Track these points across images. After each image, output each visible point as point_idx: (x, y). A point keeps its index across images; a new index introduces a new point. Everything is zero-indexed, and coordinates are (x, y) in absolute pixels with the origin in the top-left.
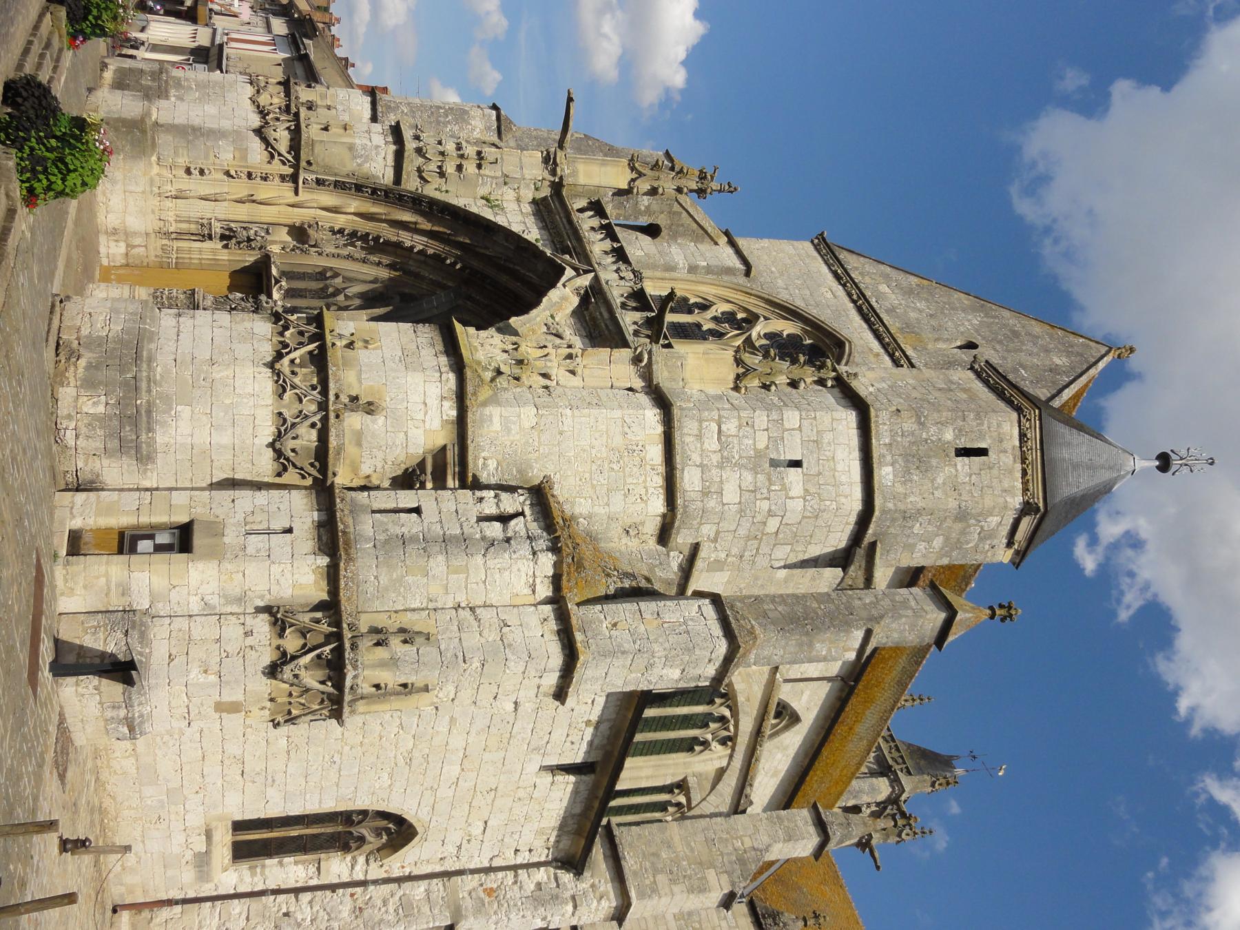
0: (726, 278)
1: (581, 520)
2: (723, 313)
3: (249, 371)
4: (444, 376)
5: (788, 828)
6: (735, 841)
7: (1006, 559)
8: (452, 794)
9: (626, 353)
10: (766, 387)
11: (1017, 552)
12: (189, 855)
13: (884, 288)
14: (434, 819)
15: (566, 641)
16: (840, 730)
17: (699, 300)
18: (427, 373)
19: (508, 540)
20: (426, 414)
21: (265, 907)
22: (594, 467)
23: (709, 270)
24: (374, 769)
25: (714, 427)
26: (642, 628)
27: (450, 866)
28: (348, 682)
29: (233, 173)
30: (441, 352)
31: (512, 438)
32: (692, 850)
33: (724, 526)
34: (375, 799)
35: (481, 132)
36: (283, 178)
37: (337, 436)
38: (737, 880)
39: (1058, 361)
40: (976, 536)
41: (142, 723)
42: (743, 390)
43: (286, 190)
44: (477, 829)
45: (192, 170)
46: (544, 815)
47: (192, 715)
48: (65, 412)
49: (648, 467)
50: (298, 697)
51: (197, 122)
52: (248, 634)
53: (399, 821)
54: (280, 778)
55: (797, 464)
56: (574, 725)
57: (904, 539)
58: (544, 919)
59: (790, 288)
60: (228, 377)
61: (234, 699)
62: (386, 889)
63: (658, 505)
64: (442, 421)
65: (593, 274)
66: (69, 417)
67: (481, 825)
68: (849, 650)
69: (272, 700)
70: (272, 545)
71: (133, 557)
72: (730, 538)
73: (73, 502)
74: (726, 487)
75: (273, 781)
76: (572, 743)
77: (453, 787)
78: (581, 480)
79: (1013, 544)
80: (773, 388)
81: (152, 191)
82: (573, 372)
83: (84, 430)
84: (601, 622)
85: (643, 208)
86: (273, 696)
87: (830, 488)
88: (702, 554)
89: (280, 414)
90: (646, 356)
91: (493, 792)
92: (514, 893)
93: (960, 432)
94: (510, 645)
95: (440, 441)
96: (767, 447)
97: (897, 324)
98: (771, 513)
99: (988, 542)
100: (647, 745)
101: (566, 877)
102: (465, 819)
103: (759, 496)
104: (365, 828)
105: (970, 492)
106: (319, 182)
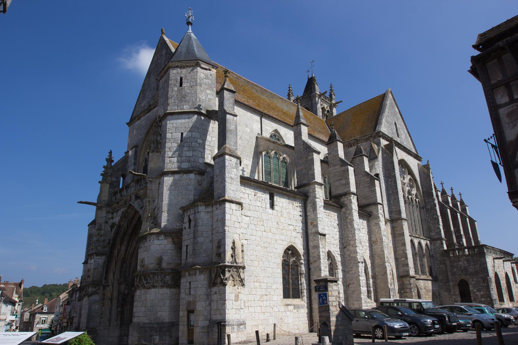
0: (138, 154)
1: (196, 198)
7: (215, 71)
10: (161, 143)
11: (213, 68)
12: (295, 311)
13: (143, 105)
17: (144, 161)
20: (163, 244)
22: (180, 194)
26: (220, 180)
28: (230, 264)
29: (102, 305)
34: (278, 257)
36: (104, 288)
37: (168, 270)
39: (164, 53)
40: (207, 80)
41: (240, 322)
43: (109, 289)
44: (292, 227)
46: (287, 208)
47: (238, 308)
51: (86, 315)
52: (216, 293)
54: (269, 285)
56: (256, 200)
57: (207, 102)
63: (192, 176)
64: (165, 239)
65: (131, 195)
68: (233, 119)
69: (235, 285)
75: (270, 286)
77: (276, 235)
81: (108, 329)
82: (154, 201)
85: (116, 179)
89: (161, 286)
93: (175, 85)
94: (222, 219)
96: (177, 143)
97: (152, 101)
99: (209, 76)
102: (288, 231)
105: (193, 82)
106: (106, 278)
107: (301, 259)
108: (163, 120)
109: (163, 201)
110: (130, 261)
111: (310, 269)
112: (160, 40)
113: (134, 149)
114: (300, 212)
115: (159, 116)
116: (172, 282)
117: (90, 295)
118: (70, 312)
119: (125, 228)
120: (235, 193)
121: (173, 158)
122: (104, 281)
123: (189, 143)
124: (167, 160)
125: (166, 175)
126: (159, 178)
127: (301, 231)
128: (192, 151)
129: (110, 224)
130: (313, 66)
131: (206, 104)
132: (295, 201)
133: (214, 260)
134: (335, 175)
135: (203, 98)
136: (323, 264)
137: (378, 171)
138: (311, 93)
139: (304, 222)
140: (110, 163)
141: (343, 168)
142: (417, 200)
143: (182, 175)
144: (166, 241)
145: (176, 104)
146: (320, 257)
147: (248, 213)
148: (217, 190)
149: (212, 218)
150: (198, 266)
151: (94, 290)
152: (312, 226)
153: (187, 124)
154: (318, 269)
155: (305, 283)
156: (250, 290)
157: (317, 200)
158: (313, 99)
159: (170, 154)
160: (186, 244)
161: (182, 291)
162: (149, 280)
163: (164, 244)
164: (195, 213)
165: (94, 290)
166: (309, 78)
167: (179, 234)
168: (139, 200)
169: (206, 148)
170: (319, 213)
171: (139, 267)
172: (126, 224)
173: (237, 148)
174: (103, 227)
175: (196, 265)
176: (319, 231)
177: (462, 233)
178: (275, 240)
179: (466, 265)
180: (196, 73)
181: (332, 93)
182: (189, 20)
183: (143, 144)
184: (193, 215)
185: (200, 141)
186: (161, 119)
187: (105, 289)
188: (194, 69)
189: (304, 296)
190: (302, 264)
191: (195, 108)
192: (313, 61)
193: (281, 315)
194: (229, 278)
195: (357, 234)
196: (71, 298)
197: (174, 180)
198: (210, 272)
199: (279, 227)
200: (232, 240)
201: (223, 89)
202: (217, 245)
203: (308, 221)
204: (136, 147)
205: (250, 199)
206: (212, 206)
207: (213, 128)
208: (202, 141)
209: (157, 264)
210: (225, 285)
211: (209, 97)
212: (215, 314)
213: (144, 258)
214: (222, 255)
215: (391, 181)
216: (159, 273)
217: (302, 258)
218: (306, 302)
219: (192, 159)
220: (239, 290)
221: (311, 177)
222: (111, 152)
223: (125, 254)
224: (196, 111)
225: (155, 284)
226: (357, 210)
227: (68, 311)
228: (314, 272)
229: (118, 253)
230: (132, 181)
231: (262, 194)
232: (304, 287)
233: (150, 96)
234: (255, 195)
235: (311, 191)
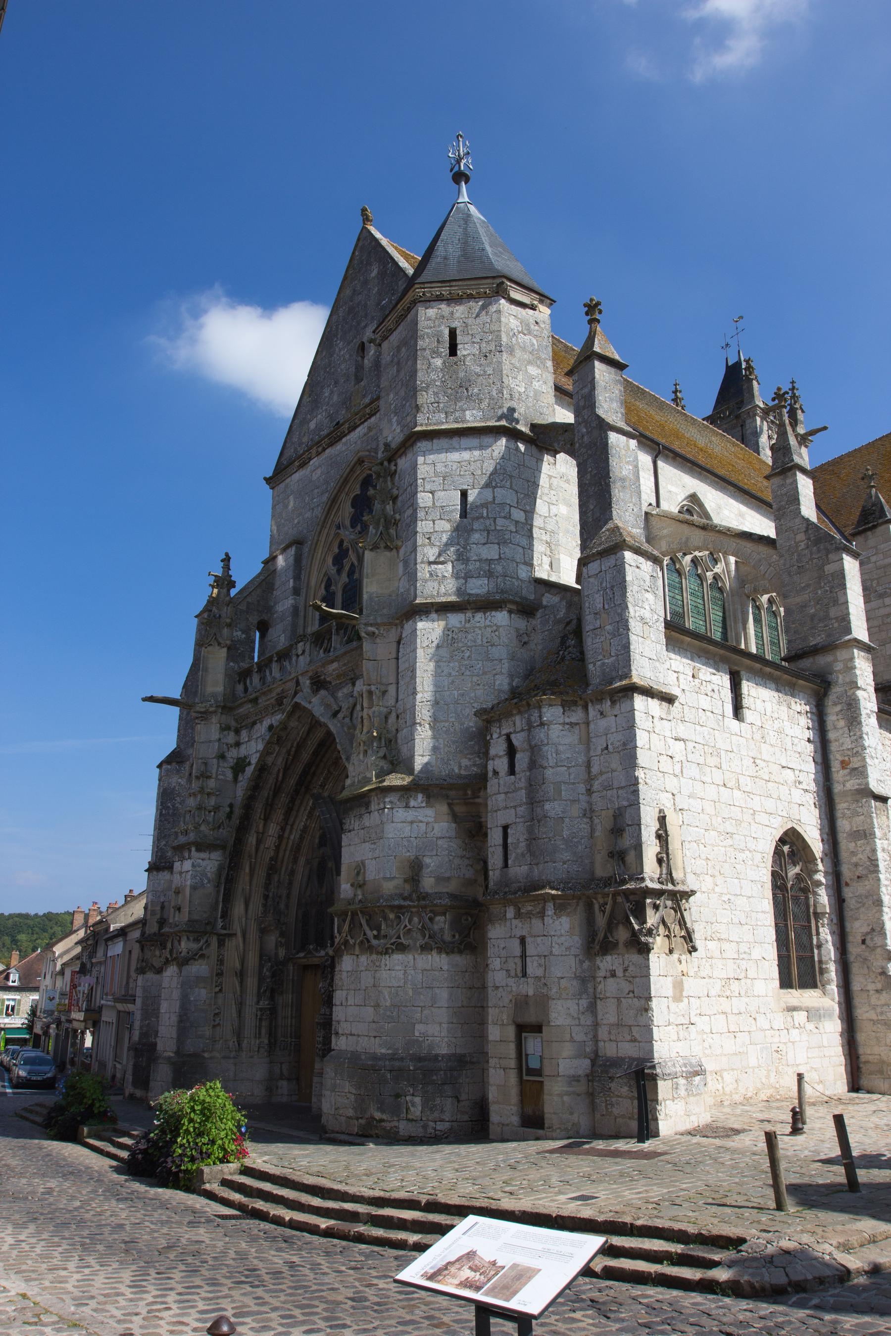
0: (304, 562)
1: (514, 684)
2: (334, 564)
3: (384, 974)
5: (788, 501)
6: (800, 548)
10: (396, 523)
11: (541, 302)
12: (810, 1026)
13: (312, 425)
15: (620, 695)
16: (701, 459)
17: (323, 586)
18: (385, 820)
20: (421, 822)
22: (468, 673)
26: (608, 627)
28: (657, 886)
29: (217, 989)
30: (367, 808)
32: (808, 586)
34: (763, 865)
35: (181, 778)
37: (440, 899)
38: (834, 546)
39: (374, 273)
40: (527, 337)
41: (691, 1065)
44: (789, 775)
45: (217, 1022)
46: (776, 715)
47: (684, 1021)
48: (421, 1130)
49: (467, 625)
51: (174, 1019)
52: (613, 974)
53: (782, 841)
54: (744, 947)
56: (697, 690)
57: (531, 400)
58: (869, 717)
63: (501, 617)
64: (427, 806)
65: (300, 678)
66: (425, 1127)
68: (628, 446)
69: (671, 951)
70: (535, 954)
71: (547, 1071)
73: (499, 1123)
74: (484, 556)
75: (745, 953)
77: (752, 796)
81: (234, 1058)
82: (384, 693)
83: (436, 1114)
84: (603, 664)
85: (244, 636)
86: (667, 952)
90: (370, 629)
91: (758, 761)
92: (848, 743)
93: (436, 353)
94: (624, 744)
95: (444, 808)
96: (449, 521)
99: (532, 327)
102: (781, 786)
105: (488, 342)
106: (225, 915)
107: (817, 871)
108: (400, 456)
109: (415, 693)
110: (290, 865)
111: (844, 901)
112: (359, 239)
113: (292, 551)
114: (808, 728)
115: (387, 445)
116: (454, 936)
117: (183, 962)
118: (90, 997)
119: (279, 770)
120: (655, 668)
121: (440, 566)
122: (220, 923)
123: (488, 522)
124: (423, 571)
125: (420, 615)
126: (396, 625)
127: (813, 787)
128: (499, 544)
129: (231, 760)
130: (739, 330)
131: (528, 408)
132: (793, 696)
133: (600, 872)
134: (883, 624)
135: (519, 389)
138: (741, 404)
139: (819, 760)
140: (225, 590)
143: (469, 614)
144: (430, 812)
145: (441, 405)
146: (877, 866)
147: (682, 730)
148: (600, 657)
149: (587, 741)
150: (552, 888)
151: (194, 946)
152: (846, 771)
153: (478, 464)
154: (870, 902)
155: (830, 943)
157: (860, 693)
158: (748, 421)
159: (431, 553)
160: (502, 821)
161: (495, 963)
162: (383, 927)
164: (530, 727)
165: (194, 946)
166: (730, 364)
167: (469, 792)
168: (323, 692)
169: (535, 536)
170: (867, 734)
171: (345, 889)
172: (280, 761)
174: (214, 771)
175: (544, 887)
176: (871, 786)
178: (752, 811)
180: (495, 316)
181: (797, 406)
182: (460, 167)
183: (320, 533)
184: (524, 734)
185: (518, 515)
186: (396, 453)
187: (224, 945)
188: (490, 304)
189: (829, 982)
190: (818, 884)
191: (500, 419)
192: (741, 317)
193: (776, 1040)
194: (657, 928)
196: (91, 957)
197: (447, 629)
198: (589, 906)
200: (657, 810)
201: (588, 356)
203: (832, 757)
204: (298, 543)
205: (682, 687)
206: (586, 708)
207: (550, 477)
208: (522, 513)
209: (406, 881)
210: (645, 950)
212: (613, 1038)
213: (363, 862)
214: (631, 857)
216: (414, 907)
217: (820, 867)
218: (837, 999)
219: (499, 568)
220: (683, 967)
221: (836, 625)
222: (227, 560)
223: (278, 848)
224: (504, 426)
225: (403, 940)
227: (84, 988)
228: (858, 909)
229: (259, 842)
230: (297, 638)
232: (829, 953)
233: (335, 398)
234: (693, 676)
235: (839, 666)
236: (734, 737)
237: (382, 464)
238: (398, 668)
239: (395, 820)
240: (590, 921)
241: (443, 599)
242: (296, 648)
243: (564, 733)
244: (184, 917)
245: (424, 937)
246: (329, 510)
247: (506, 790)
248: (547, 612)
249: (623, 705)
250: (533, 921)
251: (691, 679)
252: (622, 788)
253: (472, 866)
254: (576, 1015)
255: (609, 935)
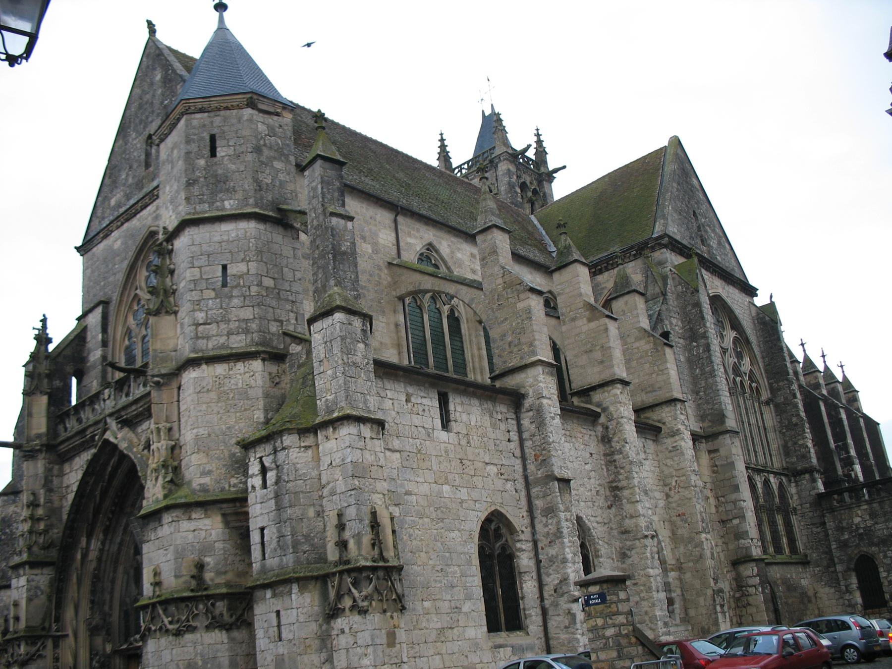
4: (175, 519)
7: (290, 116)
8: (465, 489)
9: (154, 394)
10: (174, 292)
14: (484, 499)
15: (339, 423)
19: (278, 467)
20: (201, 530)
21: (551, 605)
22: (233, 410)
23: (104, 330)
24: (447, 543)
25: (201, 328)
27: (521, 485)
28: (369, 564)
30: (160, 522)
31: (215, 469)
32: (506, 319)
33: (270, 316)
34: (470, 540)
35: (16, 506)
36: (56, 646)
38: (522, 288)
39: (159, 78)
42: (177, 309)
44: (493, 470)
47: (398, 661)
50: (382, 596)
53: (488, 521)
55: (225, 267)
57: (277, 188)
58: (553, 418)
59: (115, 271)
60: (183, 664)
61: (385, 636)
62: (539, 527)
63: (257, 365)
64: (206, 517)
67: (489, 468)
68: (346, 227)
69: (385, 611)
70: (287, 623)
72: (279, 311)
75: (456, 608)
76: (424, 410)
77: (459, 488)
78: (241, 419)
79: (277, 112)
80: (175, 287)
82: (170, 429)
84: (327, 400)
86: (381, 611)
87: (241, 243)
88: (291, 328)
89: (206, 627)
90: (156, 379)
91: (464, 461)
93: (200, 156)
94: (343, 460)
95: (218, 519)
96: (214, 290)
98: (260, 284)
99: (277, 129)
100: (454, 351)
101: (527, 403)
102: (485, 479)
103: (248, 293)
104: (494, 547)
106: (58, 620)
110: (111, 575)
121: (208, 326)
125: (193, 367)
128: (253, 306)
136: (568, 547)
137: (668, 326)
141: (593, 325)
142: (754, 385)
144: (207, 522)
146: (562, 533)
147: (396, 444)
148: (324, 395)
156: (415, 619)
157: (545, 401)
161: (260, 633)
163: (204, 528)
164: (275, 451)
166: (486, 115)
170: (551, 432)
171: (147, 589)
173: (360, 295)
176: (556, 473)
177: (853, 452)
178: (460, 500)
179: (869, 523)
184: (272, 457)
195: (637, 473)
199: (466, 470)
200: (369, 507)
202: (334, 521)
204: (105, 303)
206: (316, 434)
211: (282, 178)
215: (697, 346)
222: (44, 321)
223: (99, 559)
225: (191, 623)
226: (633, 418)
231: (422, 397)
233: (130, 181)
236: (443, 445)
237: (161, 244)
238: (179, 409)
239: (181, 530)
240: (324, 595)
241: (211, 353)
242: (103, 394)
243: (300, 454)
244: (22, 625)
245: (208, 619)
246: (128, 274)
247: (261, 501)
248: (293, 358)
249: (341, 431)
250: (285, 599)
251: (405, 403)
252: (343, 493)
253: (244, 561)
254: (319, 665)
255: (338, 604)
